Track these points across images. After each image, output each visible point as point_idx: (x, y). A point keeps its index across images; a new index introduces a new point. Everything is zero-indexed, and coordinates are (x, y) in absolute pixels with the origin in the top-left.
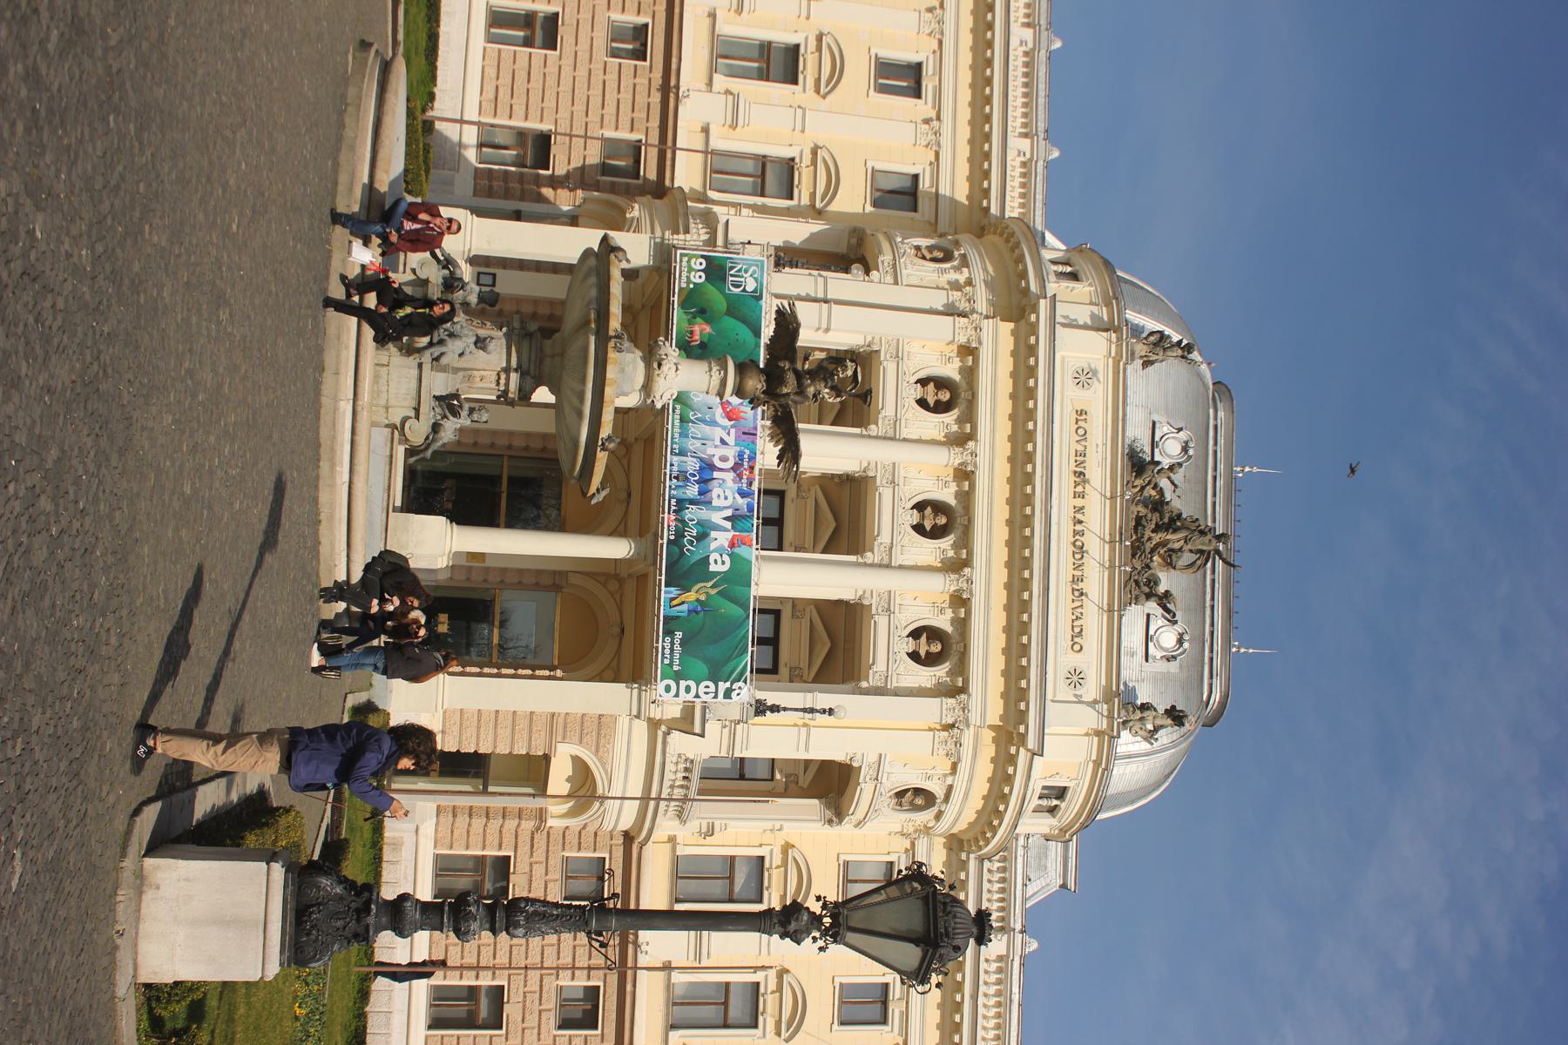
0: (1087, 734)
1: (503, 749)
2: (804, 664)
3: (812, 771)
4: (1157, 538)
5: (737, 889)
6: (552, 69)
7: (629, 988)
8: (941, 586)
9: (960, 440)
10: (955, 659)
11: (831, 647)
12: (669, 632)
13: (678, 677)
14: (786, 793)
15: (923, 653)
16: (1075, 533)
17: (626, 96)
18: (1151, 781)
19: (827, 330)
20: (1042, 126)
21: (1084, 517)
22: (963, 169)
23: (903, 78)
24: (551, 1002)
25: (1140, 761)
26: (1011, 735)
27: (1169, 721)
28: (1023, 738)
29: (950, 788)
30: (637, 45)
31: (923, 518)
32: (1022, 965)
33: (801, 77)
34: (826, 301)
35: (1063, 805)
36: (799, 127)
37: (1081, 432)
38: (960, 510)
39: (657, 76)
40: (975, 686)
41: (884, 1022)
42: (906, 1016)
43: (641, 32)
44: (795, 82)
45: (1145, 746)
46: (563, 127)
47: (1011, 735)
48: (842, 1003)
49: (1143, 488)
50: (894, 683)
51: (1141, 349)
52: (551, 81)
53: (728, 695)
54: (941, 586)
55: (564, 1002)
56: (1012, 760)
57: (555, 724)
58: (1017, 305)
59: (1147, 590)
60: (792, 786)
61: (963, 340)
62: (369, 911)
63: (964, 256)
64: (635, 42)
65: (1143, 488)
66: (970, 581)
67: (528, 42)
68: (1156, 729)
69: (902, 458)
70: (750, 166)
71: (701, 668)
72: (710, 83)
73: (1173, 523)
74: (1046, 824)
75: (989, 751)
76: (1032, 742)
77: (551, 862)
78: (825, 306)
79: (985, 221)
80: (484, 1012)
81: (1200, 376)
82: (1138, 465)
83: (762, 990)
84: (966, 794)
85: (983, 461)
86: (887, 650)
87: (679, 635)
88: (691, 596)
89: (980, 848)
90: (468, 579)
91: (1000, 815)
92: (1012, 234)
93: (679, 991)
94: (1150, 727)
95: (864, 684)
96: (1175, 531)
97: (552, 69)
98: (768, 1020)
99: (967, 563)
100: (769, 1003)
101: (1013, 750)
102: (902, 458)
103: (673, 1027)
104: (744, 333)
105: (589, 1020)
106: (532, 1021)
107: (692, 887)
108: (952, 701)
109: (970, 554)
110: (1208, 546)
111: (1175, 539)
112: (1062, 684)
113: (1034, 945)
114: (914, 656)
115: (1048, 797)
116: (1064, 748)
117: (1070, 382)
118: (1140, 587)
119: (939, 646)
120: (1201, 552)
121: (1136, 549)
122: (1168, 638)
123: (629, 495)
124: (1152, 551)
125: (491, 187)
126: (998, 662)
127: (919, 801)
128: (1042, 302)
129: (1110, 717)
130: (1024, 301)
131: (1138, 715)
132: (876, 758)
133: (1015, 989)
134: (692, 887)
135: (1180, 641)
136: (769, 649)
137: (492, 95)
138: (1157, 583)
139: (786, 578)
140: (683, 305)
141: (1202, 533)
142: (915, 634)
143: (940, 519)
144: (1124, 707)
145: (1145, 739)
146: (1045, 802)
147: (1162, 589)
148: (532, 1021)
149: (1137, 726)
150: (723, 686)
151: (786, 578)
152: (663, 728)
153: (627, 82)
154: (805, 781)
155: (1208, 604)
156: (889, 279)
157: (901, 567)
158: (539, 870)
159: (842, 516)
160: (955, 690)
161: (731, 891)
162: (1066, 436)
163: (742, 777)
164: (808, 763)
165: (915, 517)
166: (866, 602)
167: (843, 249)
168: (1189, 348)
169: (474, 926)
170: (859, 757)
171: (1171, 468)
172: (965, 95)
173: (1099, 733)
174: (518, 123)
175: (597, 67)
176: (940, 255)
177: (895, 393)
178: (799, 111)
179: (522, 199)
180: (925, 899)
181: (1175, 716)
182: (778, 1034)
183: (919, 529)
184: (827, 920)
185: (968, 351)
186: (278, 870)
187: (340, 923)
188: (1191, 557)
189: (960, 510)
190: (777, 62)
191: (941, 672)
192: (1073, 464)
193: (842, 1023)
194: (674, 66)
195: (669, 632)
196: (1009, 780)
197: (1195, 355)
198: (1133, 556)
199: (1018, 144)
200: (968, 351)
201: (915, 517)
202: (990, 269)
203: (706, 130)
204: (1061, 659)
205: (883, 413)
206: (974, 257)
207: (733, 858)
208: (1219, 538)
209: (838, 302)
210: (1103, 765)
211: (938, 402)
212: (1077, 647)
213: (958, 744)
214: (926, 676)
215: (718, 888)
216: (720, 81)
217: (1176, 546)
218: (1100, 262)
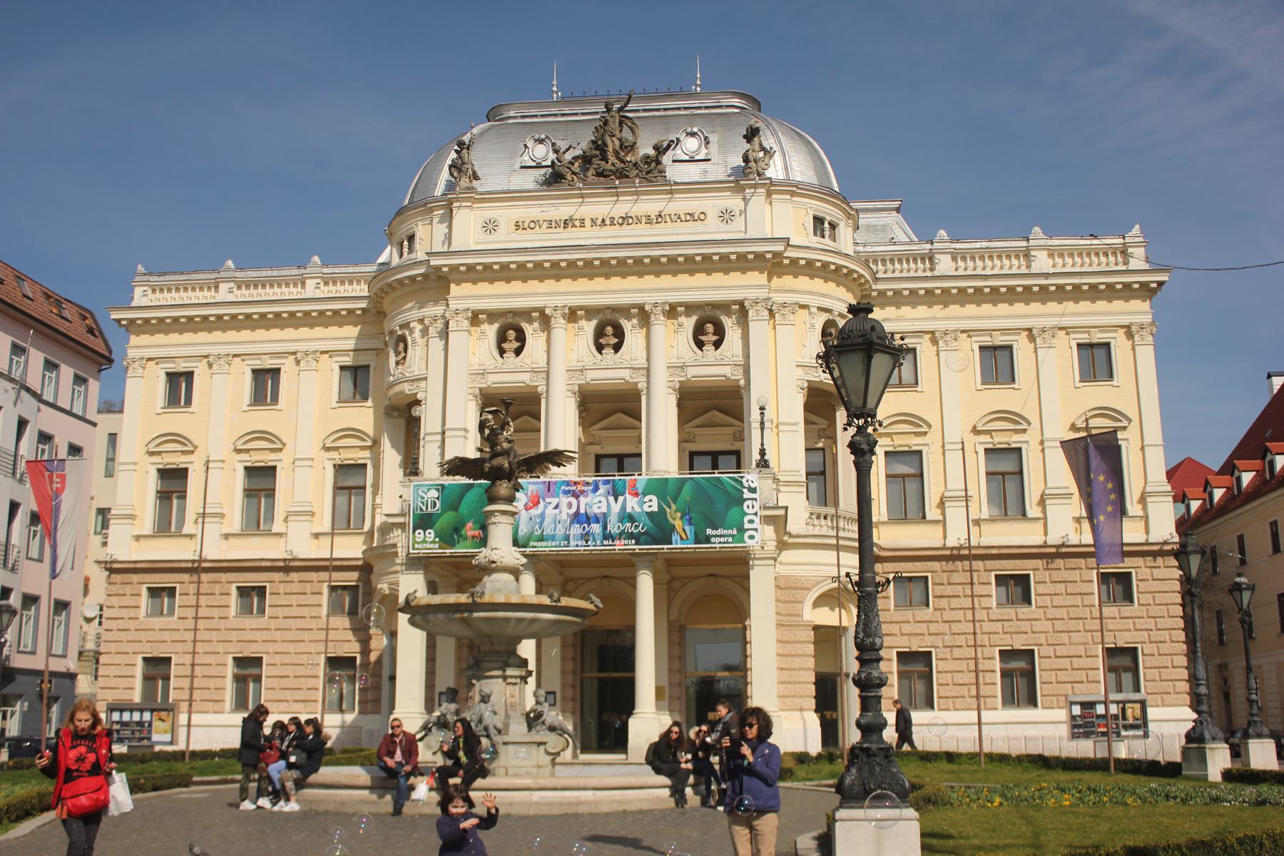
0: (771, 203)
1: (811, 663)
3: (813, 418)
4: (612, 159)
5: (912, 471)
6: (277, 659)
7: (995, 551)
8: (661, 327)
9: (545, 321)
10: (718, 312)
11: (715, 412)
12: (708, 539)
13: (742, 530)
15: (715, 338)
16: (612, 224)
17: (294, 600)
18: (805, 149)
19: (466, 430)
20: (295, 272)
21: (597, 218)
22: (334, 331)
23: (265, 383)
24: (1010, 612)
25: (789, 159)
26: (774, 263)
27: (756, 139)
28: (777, 255)
29: (820, 309)
30: (254, 593)
31: (608, 345)
32: (958, 241)
33: (270, 464)
34: (444, 433)
35: (828, 218)
36: (309, 463)
37: (532, 225)
38: (601, 316)
39: (277, 576)
40: (737, 295)
41: (1010, 348)
42: (1004, 331)
43: (244, 592)
44: (274, 468)
45: (778, 157)
47: (774, 263)
48: (997, 382)
49: (574, 173)
50: (740, 359)
51: (464, 182)
52: (287, 659)
53: (753, 490)
54: (661, 327)
55: (1010, 601)
56: (794, 261)
57: (787, 621)
58: (436, 283)
59: (653, 164)
60: (828, 433)
61: (466, 323)
62: (868, 749)
63: (401, 327)
64: (252, 596)
65: (574, 173)
66: (655, 305)
67: (258, 679)
68: (763, 149)
69: (562, 364)
70: (342, 499)
71: (734, 511)
72: (280, 535)
73: (599, 147)
74: (844, 231)
75: (788, 281)
76: (779, 247)
77: (899, 619)
78: (447, 433)
79: (373, 311)
80: (1021, 664)
81: (482, 133)
82: (555, 178)
83: (991, 446)
84: (824, 295)
85: (560, 301)
86: (714, 366)
87: (709, 531)
88: (678, 524)
89: (867, 281)
90: (679, 698)
91: (839, 268)
92: (381, 289)
93: (996, 512)
94: (761, 154)
95: (742, 383)
96: (606, 145)
97: (277, 659)
98: (1015, 440)
99: (641, 308)
100: (1000, 440)
101: (786, 262)
102: (562, 364)
103: (1024, 514)
105: (1023, 581)
106: (1025, 626)
107: (912, 506)
108: (751, 313)
109: (634, 306)
110: (616, 118)
111: (612, 144)
112: (732, 226)
113: (942, 232)
114: (717, 345)
115: (823, 231)
116: (785, 221)
117: (494, 236)
118: (651, 170)
119: (709, 325)
120: (621, 123)
121: (622, 175)
122: (691, 144)
123: (605, 577)
124: (623, 162)
125: (373, 701)
126: (718, 278)
128: (432, 263)
129: (755, 186)
130: (433, 277)
131: (752, 164)
132: (800, 369)
133: (978, 245)
134: (912, 506)
135: (693, 134)
136: (721, 459)
137: (301, 705)
138: (647, 157)
139: (662, 449)
140: (452, 545)
141: (606, 123)
142: (700, 345)
143: (609, 331)
144: (747, 176)
145: (771, 157)
146: (827, 233)
147: (652, 152)
148: (1025, 626)
149: (762, 164)
150: (747, 494)
151: (662, 449)
152: (786, 538)
153: (283, 600)
154: (823, 423)
155: (662, 113)
156: (423, 384)
157: (648, 360)
158: (907, 628)
159: (610, 409)
160: (742, 310)
161: (913, 476)
162: (536, 237)
163: (823, 473)
164: (807, 422)
165: (608, 351)
166: (678, 385)
167: (402, 422)
168: (461, 144)
169: (875, 674)
170: (800, 383)
171: (556, 151)
172: (275, 333)
173: (769, 194)
174: (320, 683)
175: (273, 624)
176: (401, 345)
177: (510, 374)
178: (297, 463)
179: (380, 676)
180: (840, 353)
181: (752, 134)
182: (1024, 431)
183: (617, 348)
184: (861, 422)
185: (475, 319)
186: (841, 814)
187: (877, 769)
188: (626, 130)
189: (601, 316)
190: (260, 483)
191: (728, 323)
192: (558, 230)
193: (1013, 381)
194: (269, 564)
196: (810, 263)
197: (466, 138)
198: (627, 177)
199: (311, 289)
200: (475, 319)
201: (608, 351)
202: (410, 305)
203: (317, 536)
204: (712, 229)
205: (528, 382)
206: (402, 319)
207: (888, 476)
208: (609, 110)
209: (444, 423)
210: (794, 189)
211: (517, 339)
212: (702, 217)
213: (784, 305)
214: (733, 335)
215: (912, 487)
216: (278, 526)
217: (617, 143)
218: (398, 219)
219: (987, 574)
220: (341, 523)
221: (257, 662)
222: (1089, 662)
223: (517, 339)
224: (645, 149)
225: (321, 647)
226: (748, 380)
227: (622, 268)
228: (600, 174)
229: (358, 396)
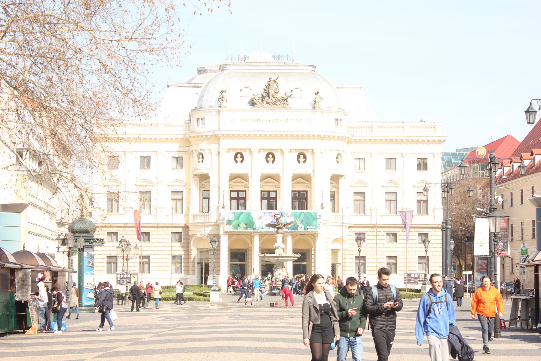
2: (305, 184)
3: (332, 182)
12: (307, 229)
13: (317, 227)
14: (337, 188)
17: (160, 237)
46: (170, 253)
53: (320, 216)
71: (315, 222)
87: (308, 227)
88: (300, 225)
104: (242, 216)
105: (395, 235)
107: (362, 210)
111: (271, 92)
127: (339, 157)
140: (237, 229)
141: (269, 85)
148: (395, 249)
150: (318, 217)
154: (334, 183)
179: (194, 263)
191: (308, 155)
195: (307, 229)
211: (241, 157)
220: (174, 211)
221: (148, 257)
222: (414, 261)
223: (241, 157)
224: (281, 94)
225: (170, 253)
226: (314, 174)
228: (268, 103)
229: (179, 167)
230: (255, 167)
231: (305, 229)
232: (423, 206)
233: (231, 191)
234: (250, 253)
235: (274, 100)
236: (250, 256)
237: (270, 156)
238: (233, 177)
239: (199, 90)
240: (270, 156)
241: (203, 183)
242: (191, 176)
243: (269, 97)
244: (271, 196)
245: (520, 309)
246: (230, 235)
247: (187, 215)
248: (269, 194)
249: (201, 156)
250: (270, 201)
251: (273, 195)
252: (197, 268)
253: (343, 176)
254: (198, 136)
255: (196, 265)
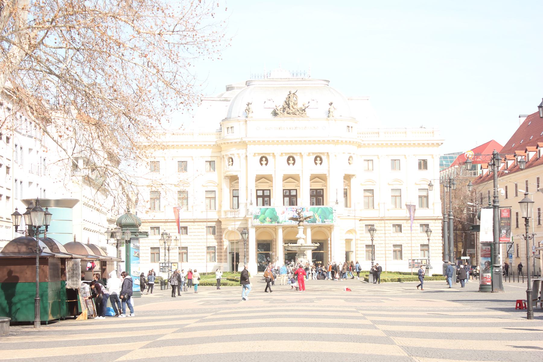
4: (291, 108)
12: (325, 222)
13: (332, 220)
14: (349, 186)
46: (205, 244)
71: (331, 216)
80: (399, 249)
88: (318, 218)
104: (268, 211)
105: (400, 226)
107: (371, 204)
111: (291, 104)
127: (351, 159)
140: (263, 222)
141: (289, 97)
150: (334, 211)
154: (347, 182)
191: (324, 158)
195: (325, 222)
219: (390, 224)
221: (186, 248)
224: (300, 106)
227: (296, 142)
228: (289, 113)
230: (278, 169)
231: (322, 222)
232: (424, 200)
233: (257, 190)
234: (274, 243)
235: (294, 110)
236: (274, 247)
237: (291, 159)
238: (259, 178)
239: (228, 104)
240: (291, 159)
241: (233, 183)
242: (223, 177)
243: (289, 108)
244: (292, 194)
245: (540, 290)
246: (257, 228)
247: (219, 211)
248: (290, 193)
249: (231, 160)
250: (291, 198)
251: (293, 193)
252: (229, 257)
253: (354, 175)
254: (228, 143)
255: (228, 254)
